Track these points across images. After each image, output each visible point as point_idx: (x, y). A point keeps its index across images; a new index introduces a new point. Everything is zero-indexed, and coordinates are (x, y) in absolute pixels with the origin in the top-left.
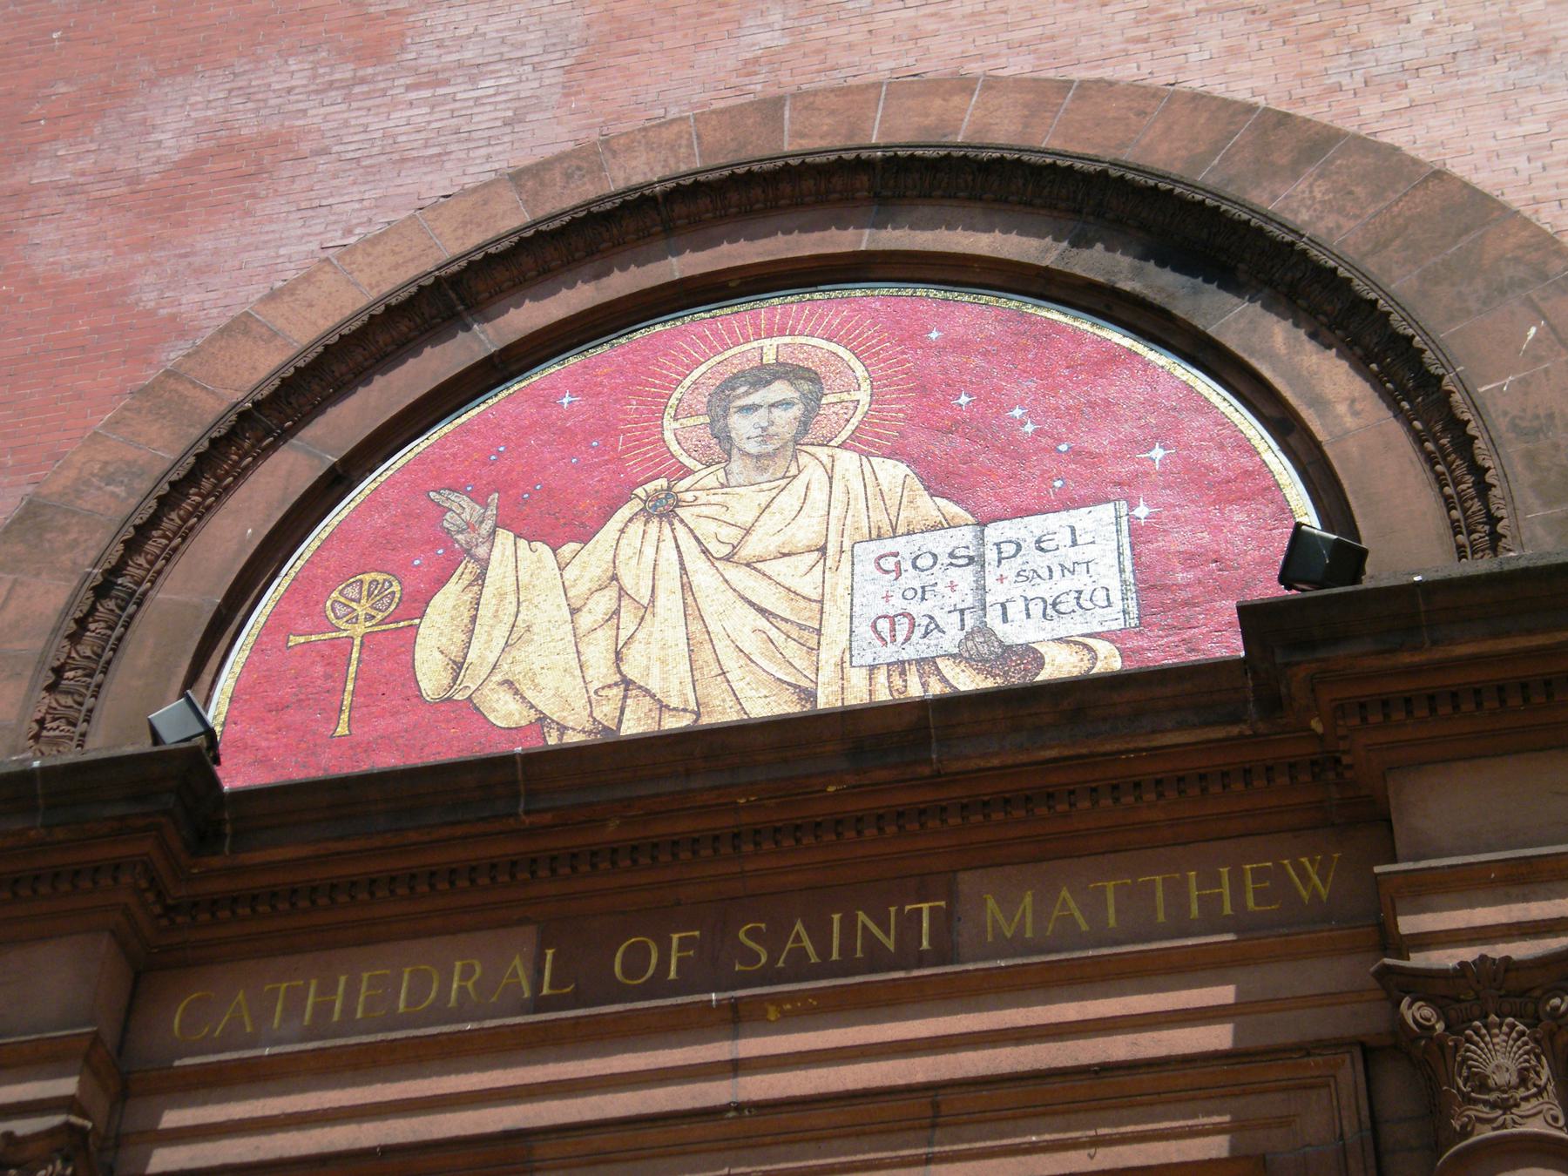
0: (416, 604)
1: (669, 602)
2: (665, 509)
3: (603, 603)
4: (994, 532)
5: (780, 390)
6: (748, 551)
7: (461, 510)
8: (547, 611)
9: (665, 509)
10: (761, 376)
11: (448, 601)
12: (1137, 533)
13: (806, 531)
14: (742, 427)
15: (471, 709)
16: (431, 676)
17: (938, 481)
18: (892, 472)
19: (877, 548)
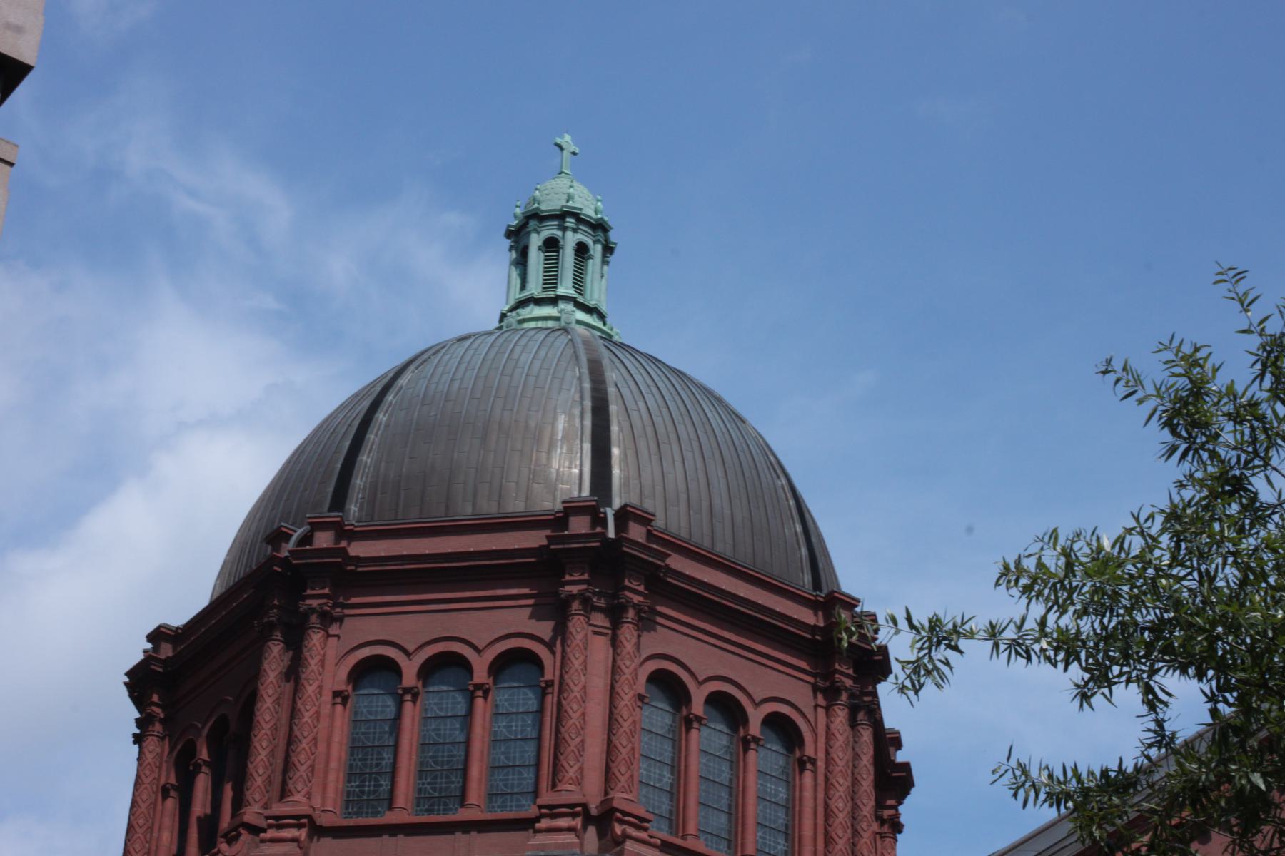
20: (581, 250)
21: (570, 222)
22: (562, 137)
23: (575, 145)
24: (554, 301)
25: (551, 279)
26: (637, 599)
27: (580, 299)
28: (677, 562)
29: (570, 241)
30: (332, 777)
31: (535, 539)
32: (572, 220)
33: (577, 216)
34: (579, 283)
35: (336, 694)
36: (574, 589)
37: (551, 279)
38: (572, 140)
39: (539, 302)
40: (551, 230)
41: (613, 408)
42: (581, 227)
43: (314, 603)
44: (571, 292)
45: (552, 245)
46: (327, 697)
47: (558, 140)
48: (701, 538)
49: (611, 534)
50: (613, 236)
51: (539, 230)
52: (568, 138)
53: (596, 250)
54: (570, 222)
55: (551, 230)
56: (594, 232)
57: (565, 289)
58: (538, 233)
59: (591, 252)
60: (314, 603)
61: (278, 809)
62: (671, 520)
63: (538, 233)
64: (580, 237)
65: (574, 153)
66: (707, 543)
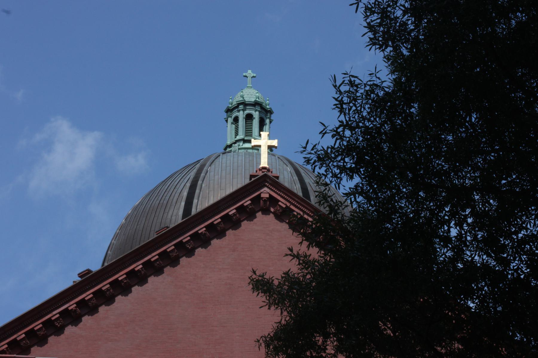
20: (249, 117)
21: (241, 107)
22: (247, 72)
23: (253, 73)
25: (237, 134)
29: (241, 115)
32: (242, 106)
38: (252, 72)
41: (303, 174)
42: (247, 107)
45: (236, 120)
47: (244, 74)
51: (231, 116)
52: (250, 71)
54: (241, 107)
56: (255, 107)
58: (231, 117)
59: (254, 116)
63: (231, 117)
64: (247, 112)
65: (253, 77)
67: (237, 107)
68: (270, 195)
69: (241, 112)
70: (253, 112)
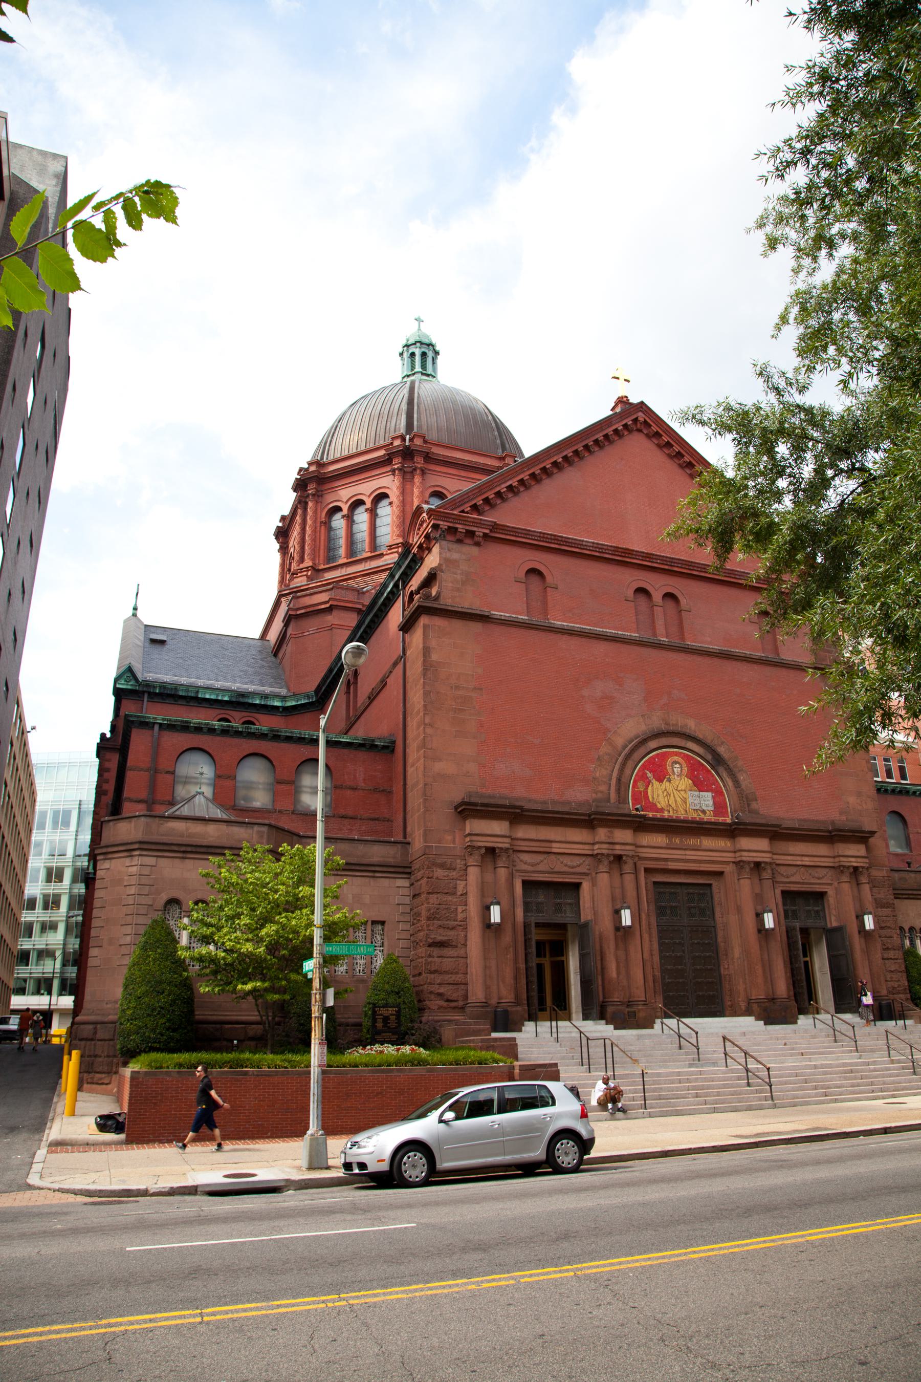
0: (647, 787)
1: (672, 795)
2: (669, 781)
3: (665, 793)
4: (701, 793)
5: (677, 766)
6: (679, 789)
7: (649, 775)
8: (660, 792)
9: (669, 781)
10: (676, 762)
11: (650, 788)
12: (713, 798)
13: (683, 788)
14: (675, 770)
15: (656, 805)
16: (651, 799)
17: (695, 784)
18: (690, 782)
19: (690, 792)
20: (424, 355)
21: (418, 344)
24: (414, 374)
25: (413, 367)
26: (419, 466)
27: (424, 372)
28: (435, 450)
29: (418, 352)
30: (322, 552)
31: (382, 452)
33: (421, 343)
34: (424, 366)
35: (321, 522)
36: (396, 467)
37: (413, 367)
39: (408, 376)
40: (412, 350)
43: (310, 492)
44: (420, 370)
45: (413, 354)
46: (319, 524)
48: (445, 439)
49: (407, 444)
50: (437, 349)
53: (430, 354)
54: (418, 344)
55: (412, 350)
57: (418, 368)
60: (310, 492)
61: (302, 566)
62: (433, 436)
66: (453, 444)
67: (415, 344)
68: (645, 420)
69: (418, 349)
70: (426, 351)
